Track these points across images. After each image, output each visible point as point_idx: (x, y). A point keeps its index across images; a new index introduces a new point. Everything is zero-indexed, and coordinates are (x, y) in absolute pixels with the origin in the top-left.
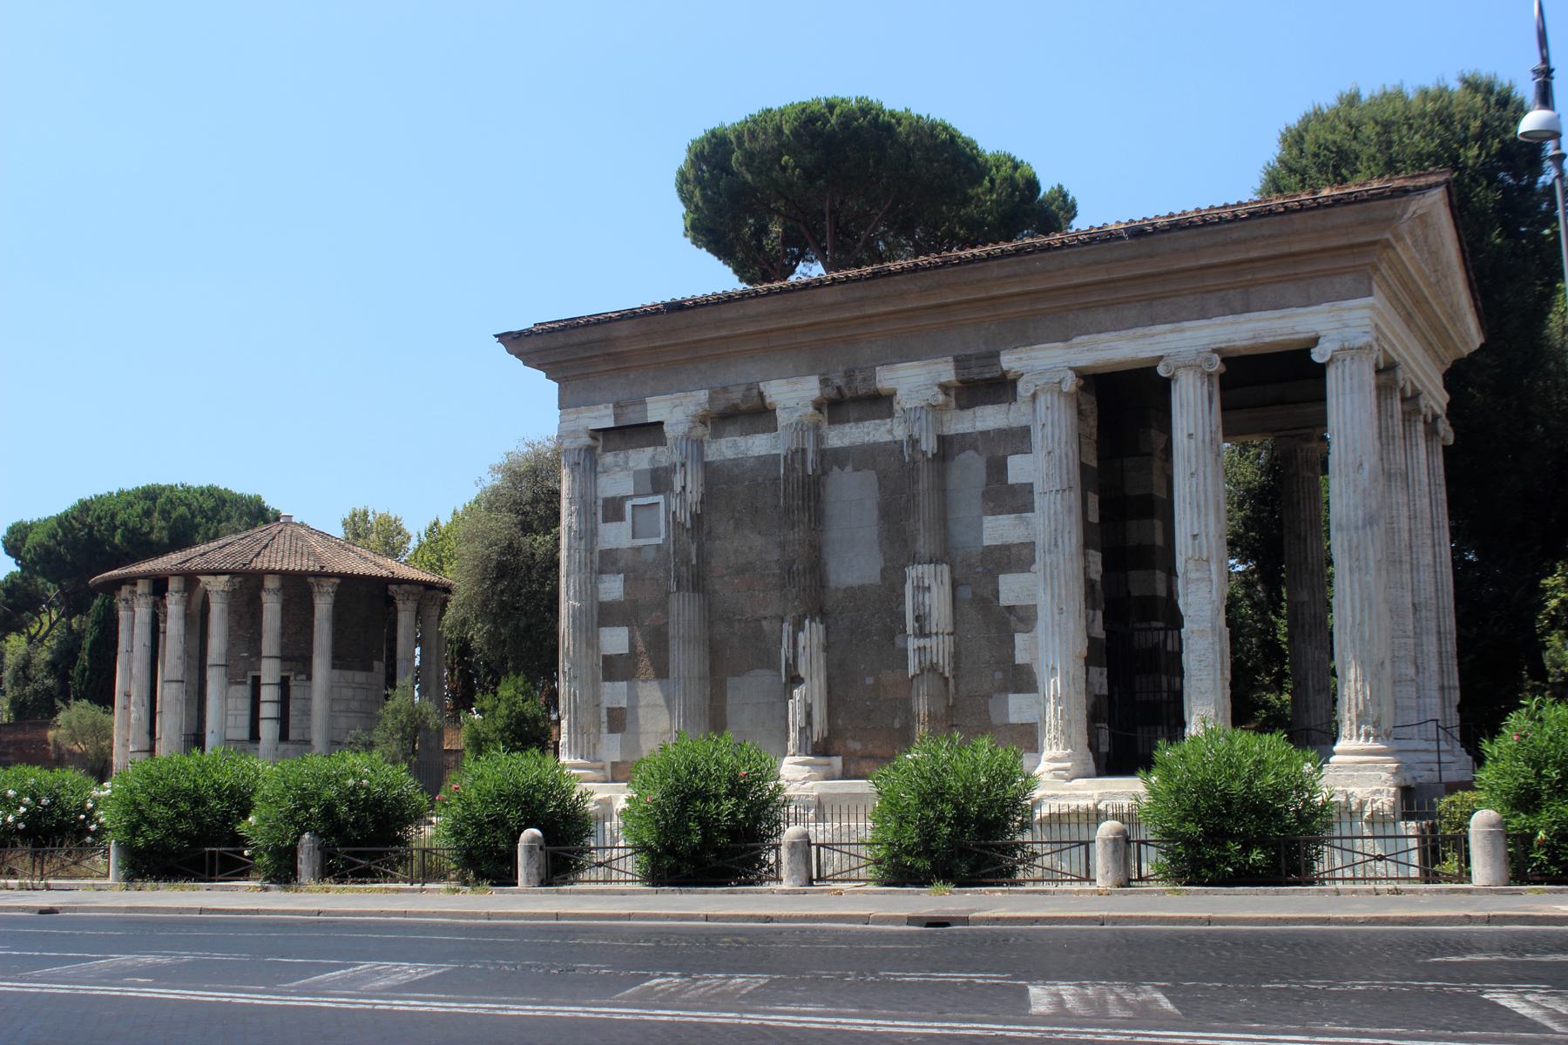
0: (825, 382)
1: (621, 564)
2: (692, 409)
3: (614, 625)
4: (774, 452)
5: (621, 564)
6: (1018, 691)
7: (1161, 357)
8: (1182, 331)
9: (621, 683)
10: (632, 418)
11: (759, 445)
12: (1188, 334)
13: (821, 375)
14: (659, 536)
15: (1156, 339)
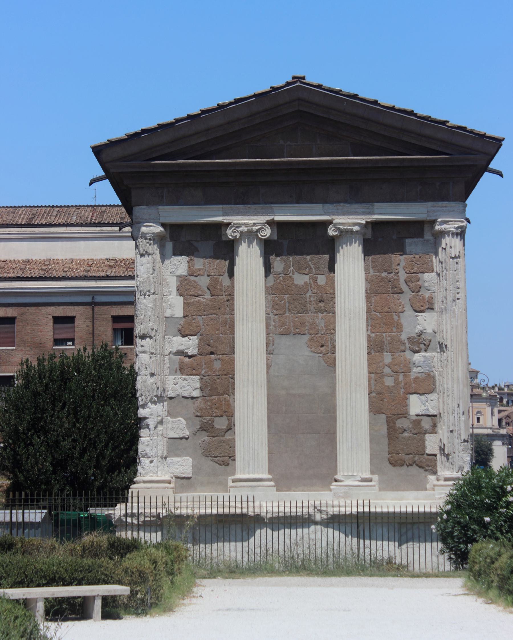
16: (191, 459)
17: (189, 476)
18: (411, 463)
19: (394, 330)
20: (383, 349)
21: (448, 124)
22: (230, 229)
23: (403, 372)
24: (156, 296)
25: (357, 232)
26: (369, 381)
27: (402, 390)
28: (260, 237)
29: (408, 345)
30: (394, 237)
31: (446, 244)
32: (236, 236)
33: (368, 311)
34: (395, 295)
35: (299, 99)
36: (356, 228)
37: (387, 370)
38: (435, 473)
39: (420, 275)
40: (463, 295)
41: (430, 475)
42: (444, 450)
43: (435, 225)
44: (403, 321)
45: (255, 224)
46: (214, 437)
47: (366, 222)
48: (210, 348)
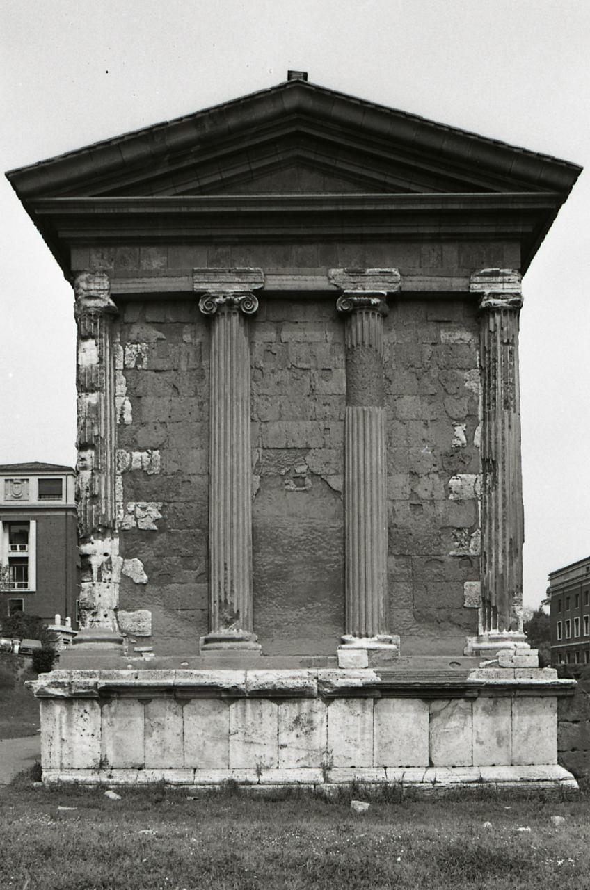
16: (150, 613)
17: (148, 635)
18: (443, 619)
22: (203, 300)
25: (376, 305)
28: (244, 311)
31: (495, 325)
32: (212, 309)
36: (374, 301)
38: (476, 633)
41: (469, 636)
42: (489, 602)
43: (481, 301)
45: (236, 294)
46: (182, 583)
47: (388, 293)
48: (176, 465)
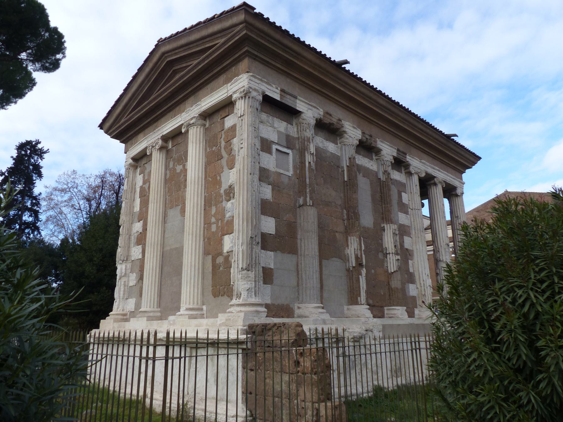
0: (363, 133)
1: (271, 179)
2: (317, 116)
3: (267, 215)
4: (337, 154)
5: (271, 179)
6: (412, 283)
7: (435, 177)
8: (439, 171)
9: (271, 252)
10: (289, 101)
11: (331, 147)
12: (440, 173)
13: (362, 130)
14: (288, 171)
15: (435, 171)
19: (218, 187)
20: (211, 205)
21: (216, 17)
23: (220, 219)
24: (127, 201)
26: (204, 231)
27: (220, 233)
29: (224, 197)
30: (219, 120)
33: (206, 177)
34: (219, 161)
35: (163, 54)
36: (192, 122)
37: (213, 220)
39: (231, 141)
40: (246, 145)
44: (223, 180)
